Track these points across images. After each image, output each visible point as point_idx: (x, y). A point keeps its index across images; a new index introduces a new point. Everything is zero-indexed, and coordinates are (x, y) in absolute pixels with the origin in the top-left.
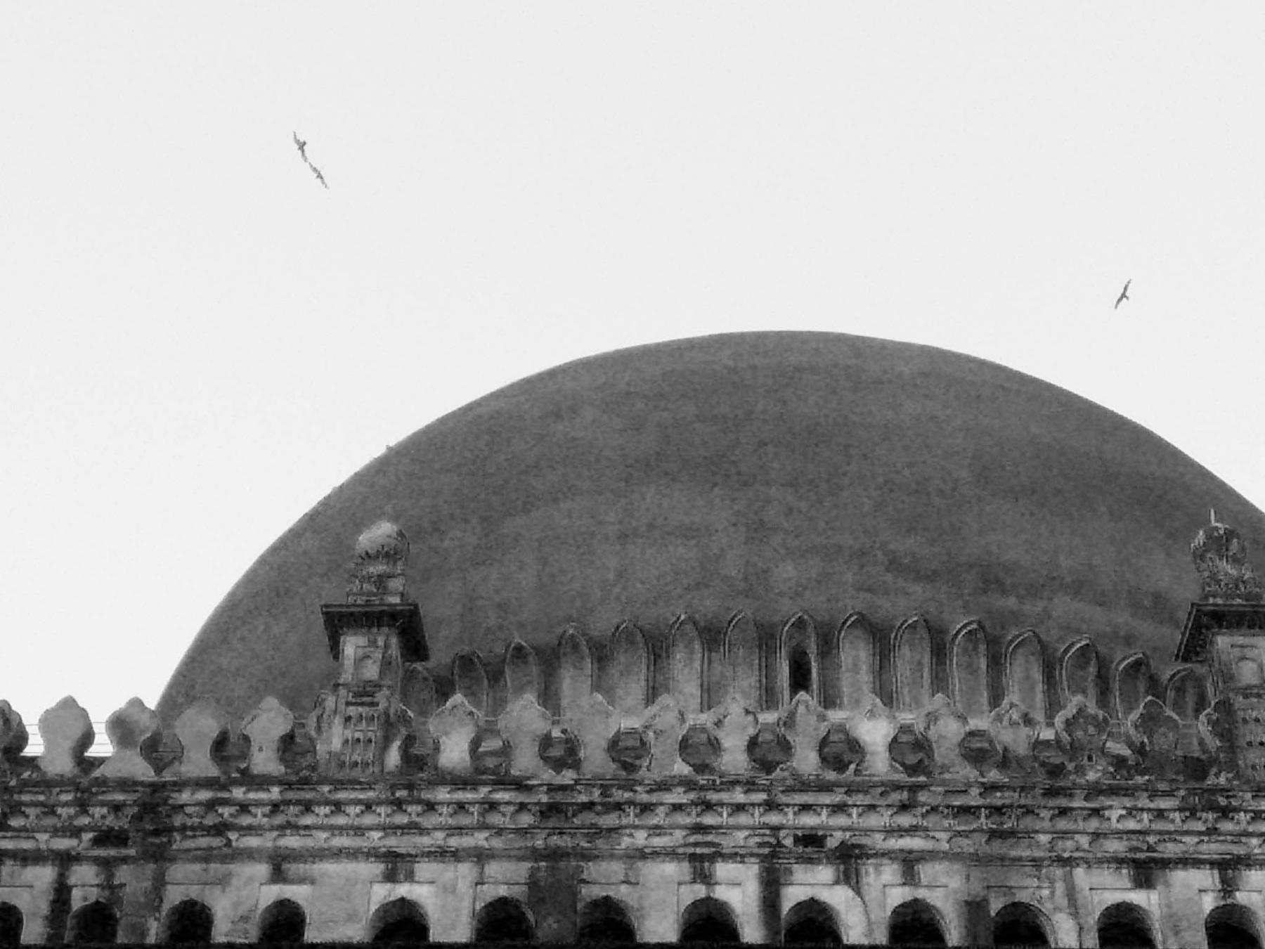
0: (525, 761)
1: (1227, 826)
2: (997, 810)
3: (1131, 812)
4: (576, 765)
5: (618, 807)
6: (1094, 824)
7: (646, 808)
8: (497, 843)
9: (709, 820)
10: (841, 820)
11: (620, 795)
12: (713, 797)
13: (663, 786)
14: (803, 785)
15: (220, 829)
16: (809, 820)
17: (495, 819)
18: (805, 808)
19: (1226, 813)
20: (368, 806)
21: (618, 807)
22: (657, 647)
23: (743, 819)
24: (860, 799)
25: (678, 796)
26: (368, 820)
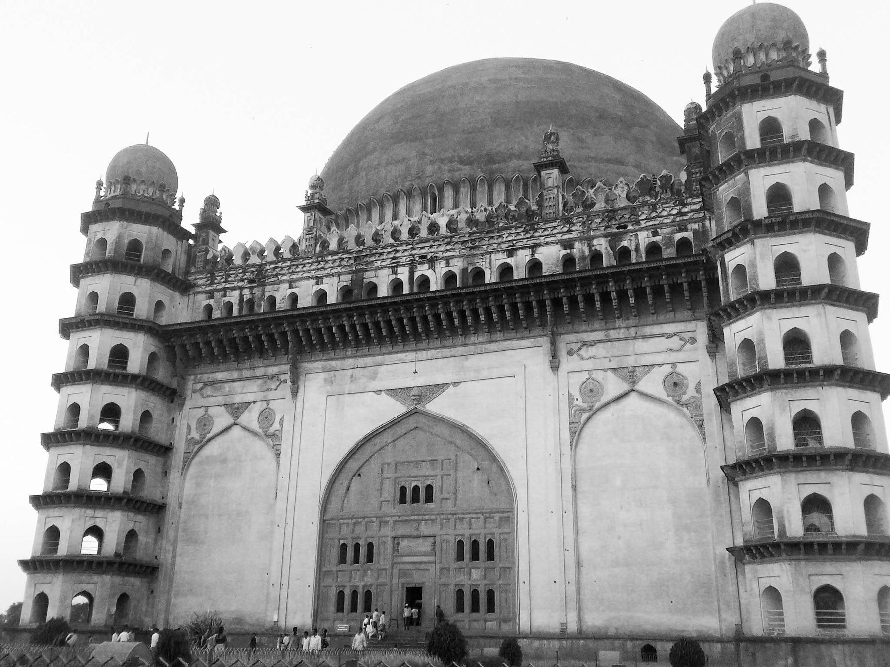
0: (351, 245)
1: (537, 234)
2: (472, 240)
3: (510, 234)
4: (363, 243)
5: (374, 255)
6: (500, 240)
7: (381, 254)
8: (343, 270)
9: (397, 255)
10: (432, 250)
11: (374, 251)
12: (398, 248)
13: (384, 247)
14: (422, 241)
15: (276, 275)
16: (423, 251)
17: (343, 263)
18: (423, 247)
19: (536, 230)
20: (312, 264)
21: (374, 255)
22: (395, 200)
23: (406, 254)
24: (437, 243)
25: (389, 250)
26: (313, 268)
